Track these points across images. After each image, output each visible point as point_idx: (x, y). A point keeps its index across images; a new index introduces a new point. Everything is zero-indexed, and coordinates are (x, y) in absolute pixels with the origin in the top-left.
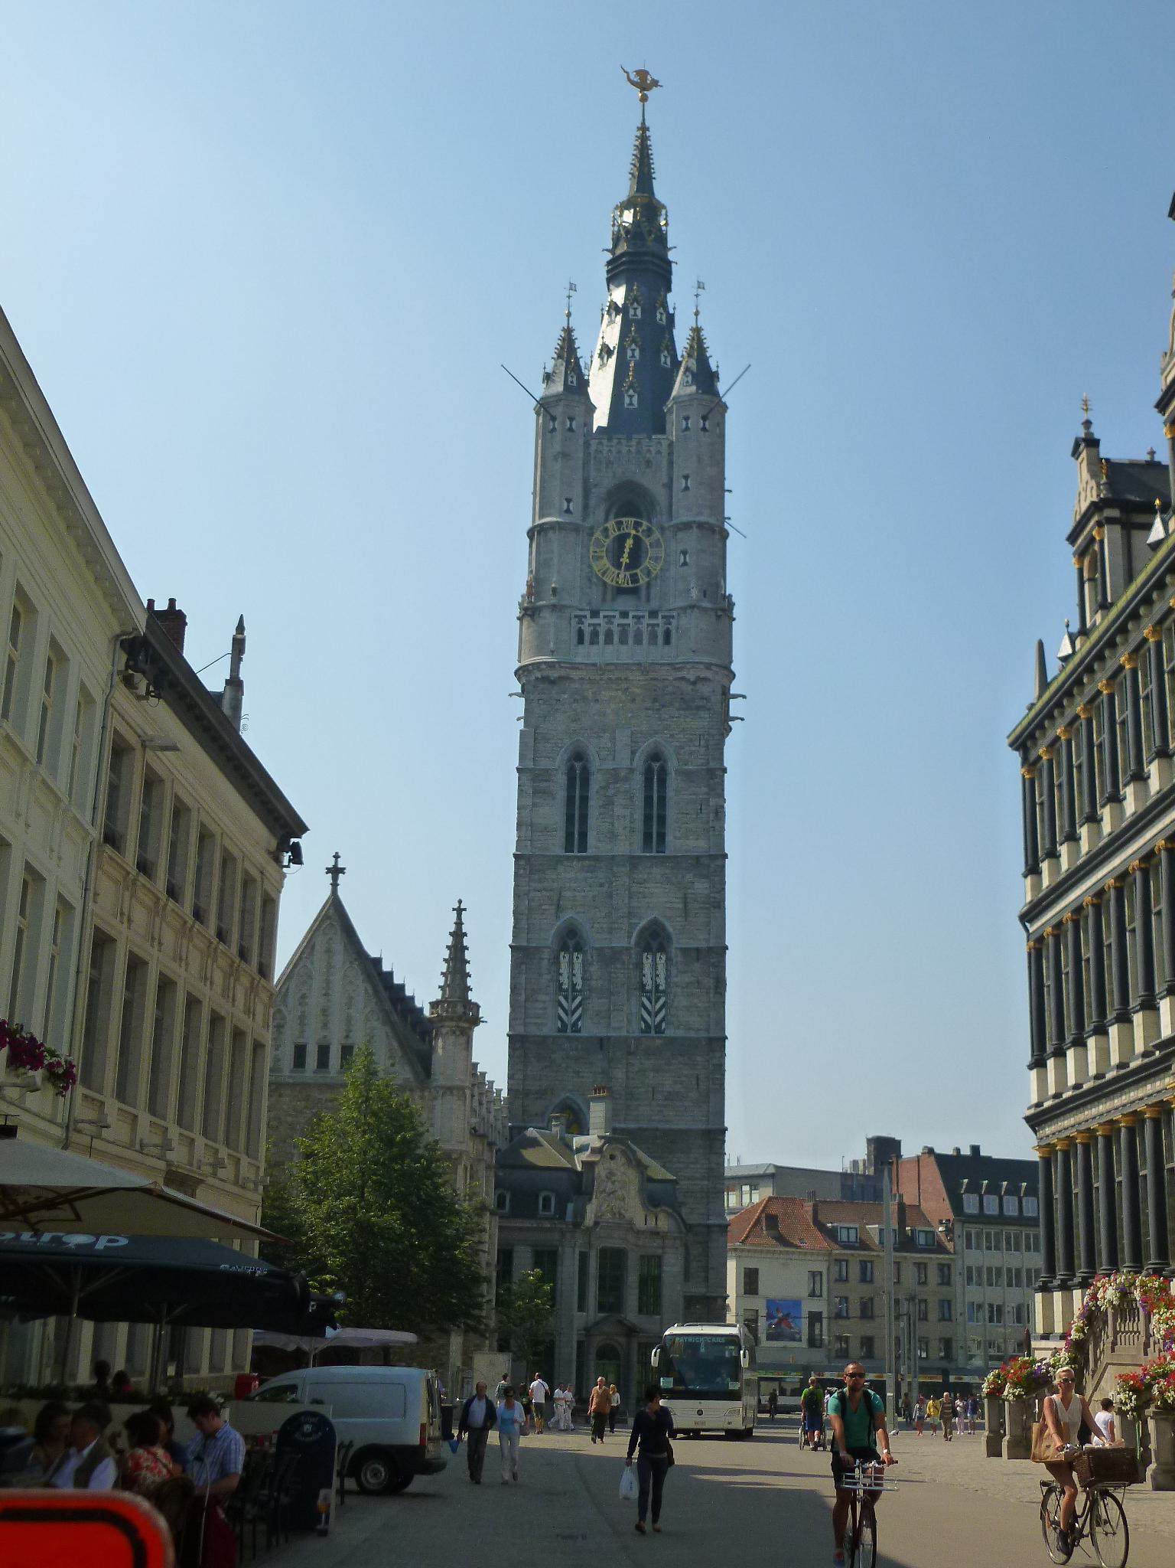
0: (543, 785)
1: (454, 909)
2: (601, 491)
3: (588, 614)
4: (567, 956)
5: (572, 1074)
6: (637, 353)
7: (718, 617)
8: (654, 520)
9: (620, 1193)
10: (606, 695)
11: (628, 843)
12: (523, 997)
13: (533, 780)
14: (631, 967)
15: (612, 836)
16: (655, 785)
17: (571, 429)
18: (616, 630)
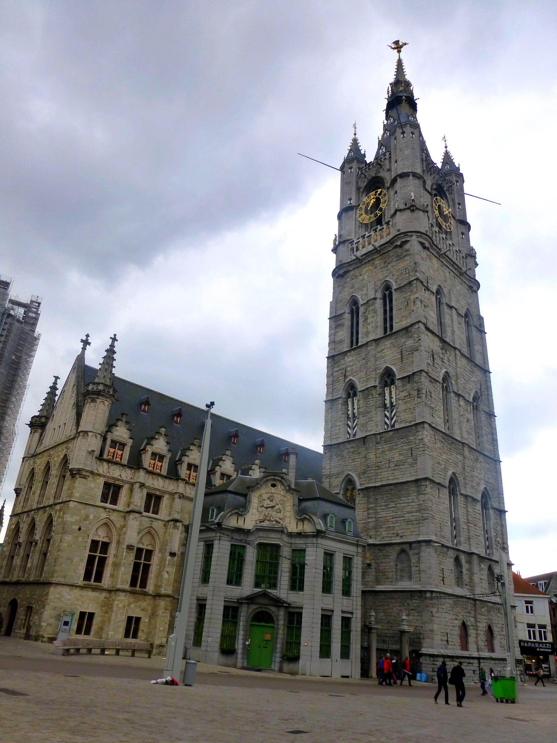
0: (339, 322)
14: (377, 396)
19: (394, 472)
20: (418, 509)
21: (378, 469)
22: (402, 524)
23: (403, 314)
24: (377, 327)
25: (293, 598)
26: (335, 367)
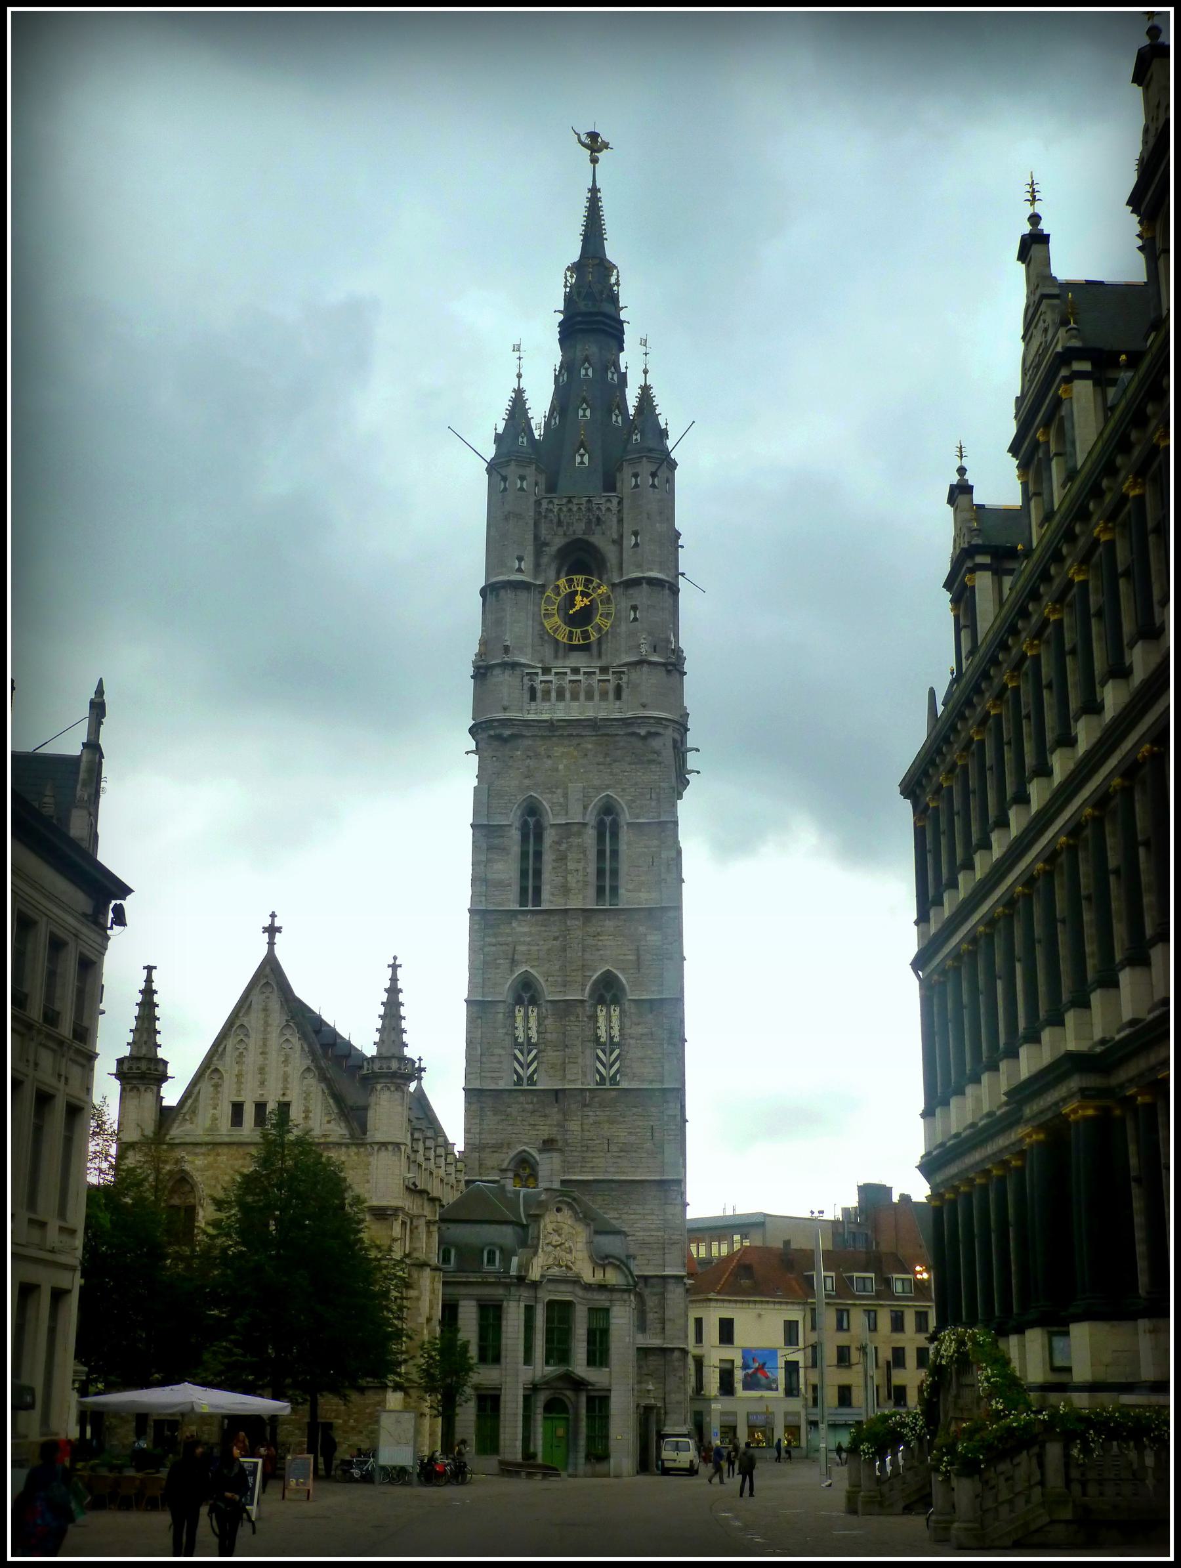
0: (496, 841)
1: (389, 966)
2: (553, 550)
3: (540, 671)
4: (522, 1010)
5: (528, 1128)
6: (588, 413)
7: (669, 672)
8: (605, 577)
9: (567, 1245)
10: (558, 751)
11: (581, 897)
14: (586, 1019)
17: (522, 489)
18: (567, 686)
19: (619, 1160)
20: (661, 1226)
23: (643, 878)
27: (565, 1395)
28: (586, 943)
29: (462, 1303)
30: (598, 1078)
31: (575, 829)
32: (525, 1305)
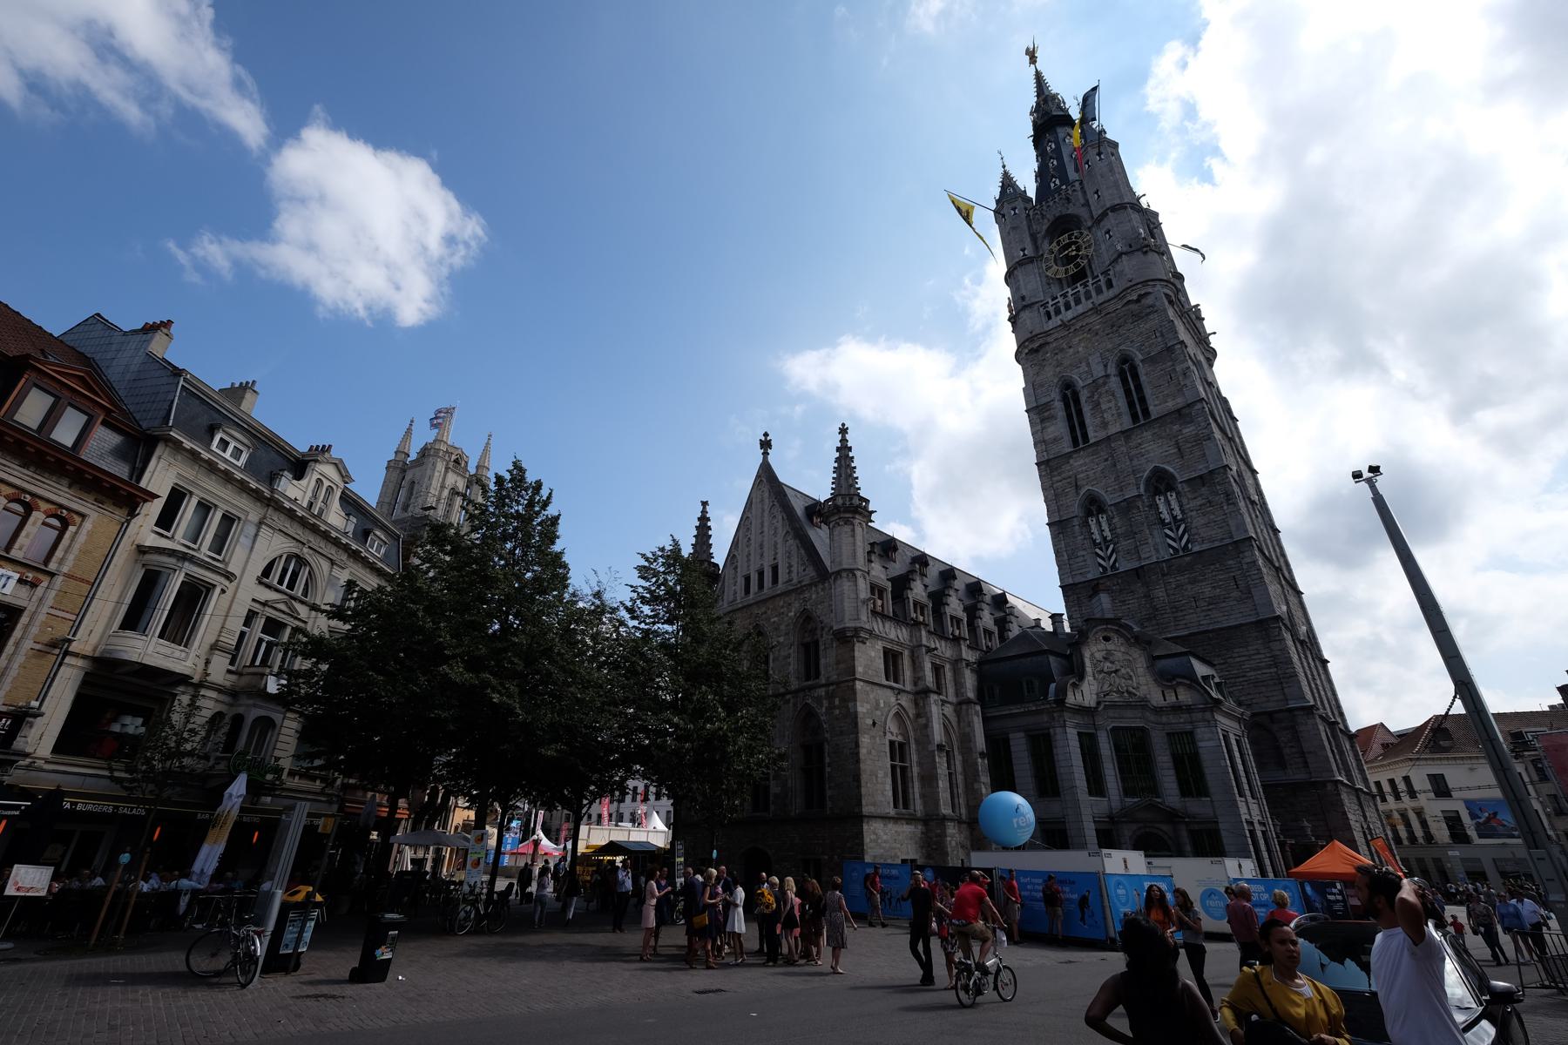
0: (1046, 414)
9: (1123, 671)
11: (1118, 424)
12: (1066, 557)
13: (1039, 413)
15: (1105, 425)
16: (1130, 379)
18: (1071, 299)
19: (1210, 613)
20: (1272, 663)
21: (1177, 612)
22: (1245, 687)
24: (1120, 415)
25: (1196, 806)
26: (1055, 476)
27: (1161, 830)
28: (1131, 454)
29: (1011, 736)
30: (1171, 551)
31: (1101, 381)
32: (1079, 733)
